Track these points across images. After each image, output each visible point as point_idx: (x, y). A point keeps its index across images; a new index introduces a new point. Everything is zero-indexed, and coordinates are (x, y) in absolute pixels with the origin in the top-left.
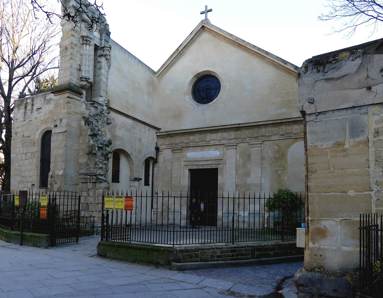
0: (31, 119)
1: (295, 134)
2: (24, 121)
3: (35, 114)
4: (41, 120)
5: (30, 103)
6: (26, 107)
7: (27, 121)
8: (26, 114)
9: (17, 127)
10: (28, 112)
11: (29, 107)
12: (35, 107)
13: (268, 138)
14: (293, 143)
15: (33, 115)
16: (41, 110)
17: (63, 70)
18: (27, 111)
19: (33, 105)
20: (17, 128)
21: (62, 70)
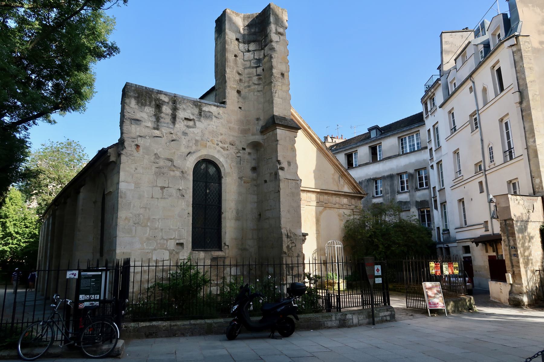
0: (173, 132)
1: (325, 203)
2: (157, 128)
3: (180, 125)
4: (197, 141)
5: (168, 103)
6: (158, 107)
7: (164, 130)
8: (162, 120)
9: (138, 134)
10: (166, 118)
11: (166, 109)
12: (181, 114)
13: (308, 203)
14: (323, 210)
15: (177, 125)
16: (191, 123)
17: (282, 99)
18: (162, 115)
19: (175, 109)
20: (140, 136)
21: (279, 97)
